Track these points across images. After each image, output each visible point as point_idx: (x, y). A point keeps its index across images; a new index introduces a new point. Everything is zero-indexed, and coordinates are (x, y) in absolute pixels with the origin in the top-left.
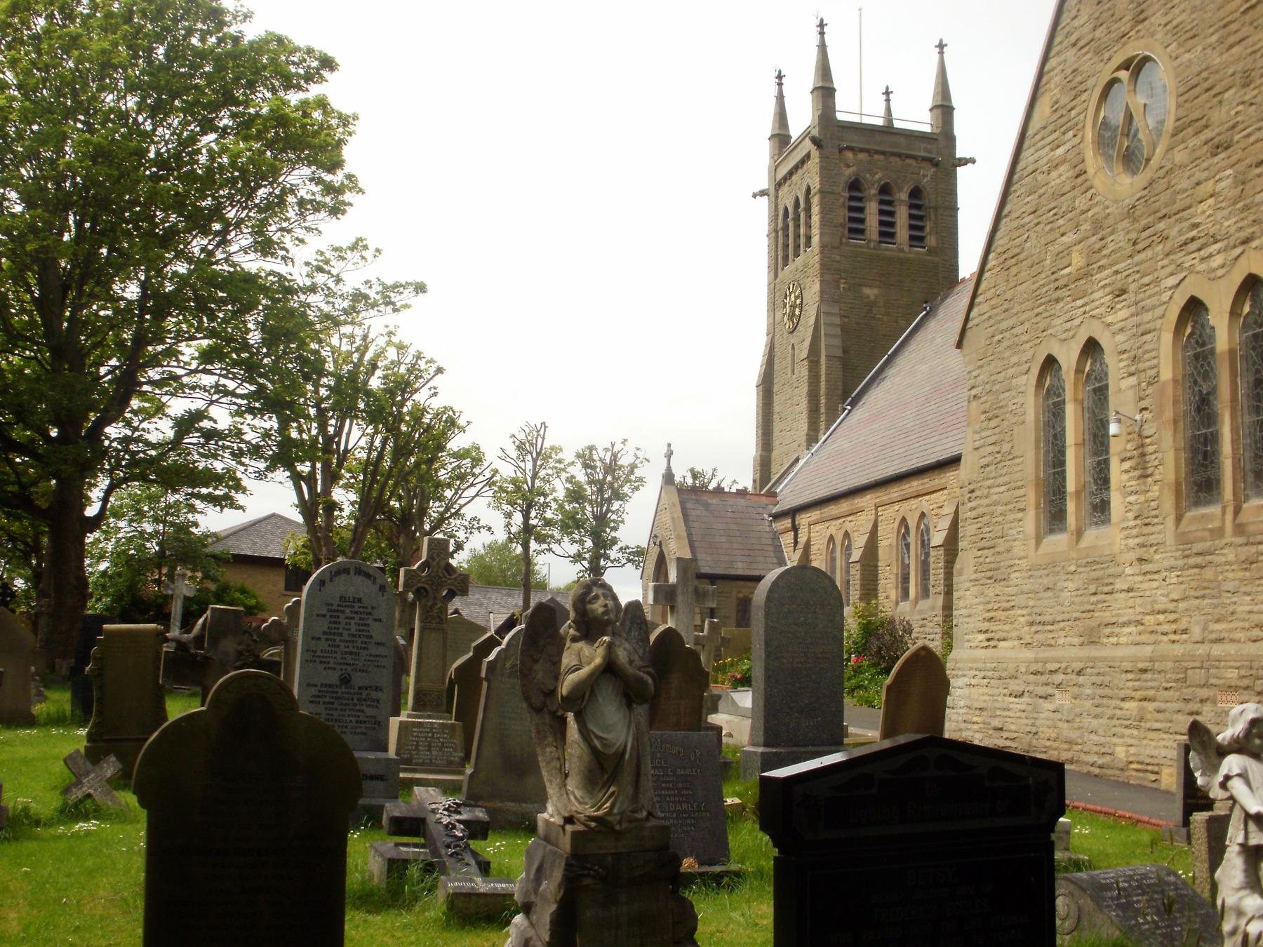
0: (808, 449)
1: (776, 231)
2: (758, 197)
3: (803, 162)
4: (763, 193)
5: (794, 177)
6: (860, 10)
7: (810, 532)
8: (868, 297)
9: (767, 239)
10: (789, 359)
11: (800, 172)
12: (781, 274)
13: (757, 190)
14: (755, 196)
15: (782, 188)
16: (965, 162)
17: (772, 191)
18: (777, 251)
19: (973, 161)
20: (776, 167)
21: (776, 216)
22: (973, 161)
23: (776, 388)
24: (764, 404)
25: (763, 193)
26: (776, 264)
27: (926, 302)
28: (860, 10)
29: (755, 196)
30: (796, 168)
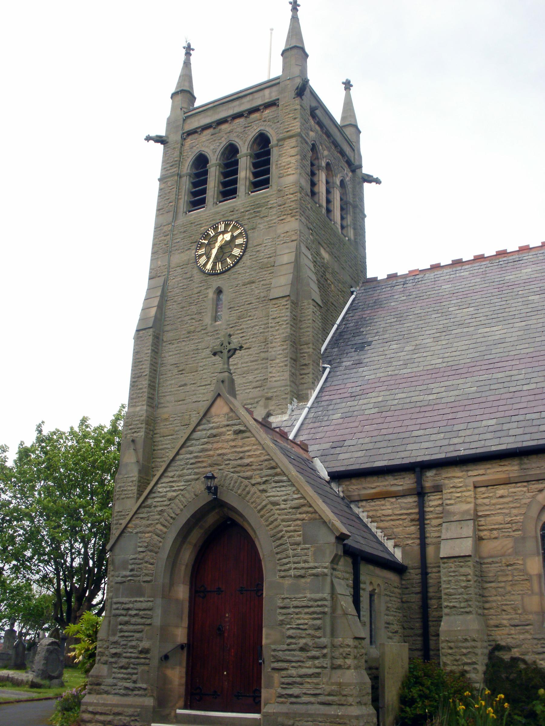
0: (291, 403)
1: (180, 176)
2: (151, 142)
3: (255, 110)
4: (159, 140)
5: (224, 127)
6: (272, 30)
7: (475, 498)
8: (323, 259)
9: (158, 183)
10: (209, 305)
11: (241, 121)
12: (182, 219)
13: (153, 134)
14: (148, 139)
15: (196, 136)
16: (369, 179)
17: (176, 138)
18: (178, 194)
19: (378, 181)
20: (187, 117)
21: (179, 163)
22: (378, 181)
23: (167, 336)
24: (153, 350)
25: (159, 140)
26: (176, 207)
27: (352, 287)
28: (272, 30)
29: (148, 139)
30: (239, 115)
